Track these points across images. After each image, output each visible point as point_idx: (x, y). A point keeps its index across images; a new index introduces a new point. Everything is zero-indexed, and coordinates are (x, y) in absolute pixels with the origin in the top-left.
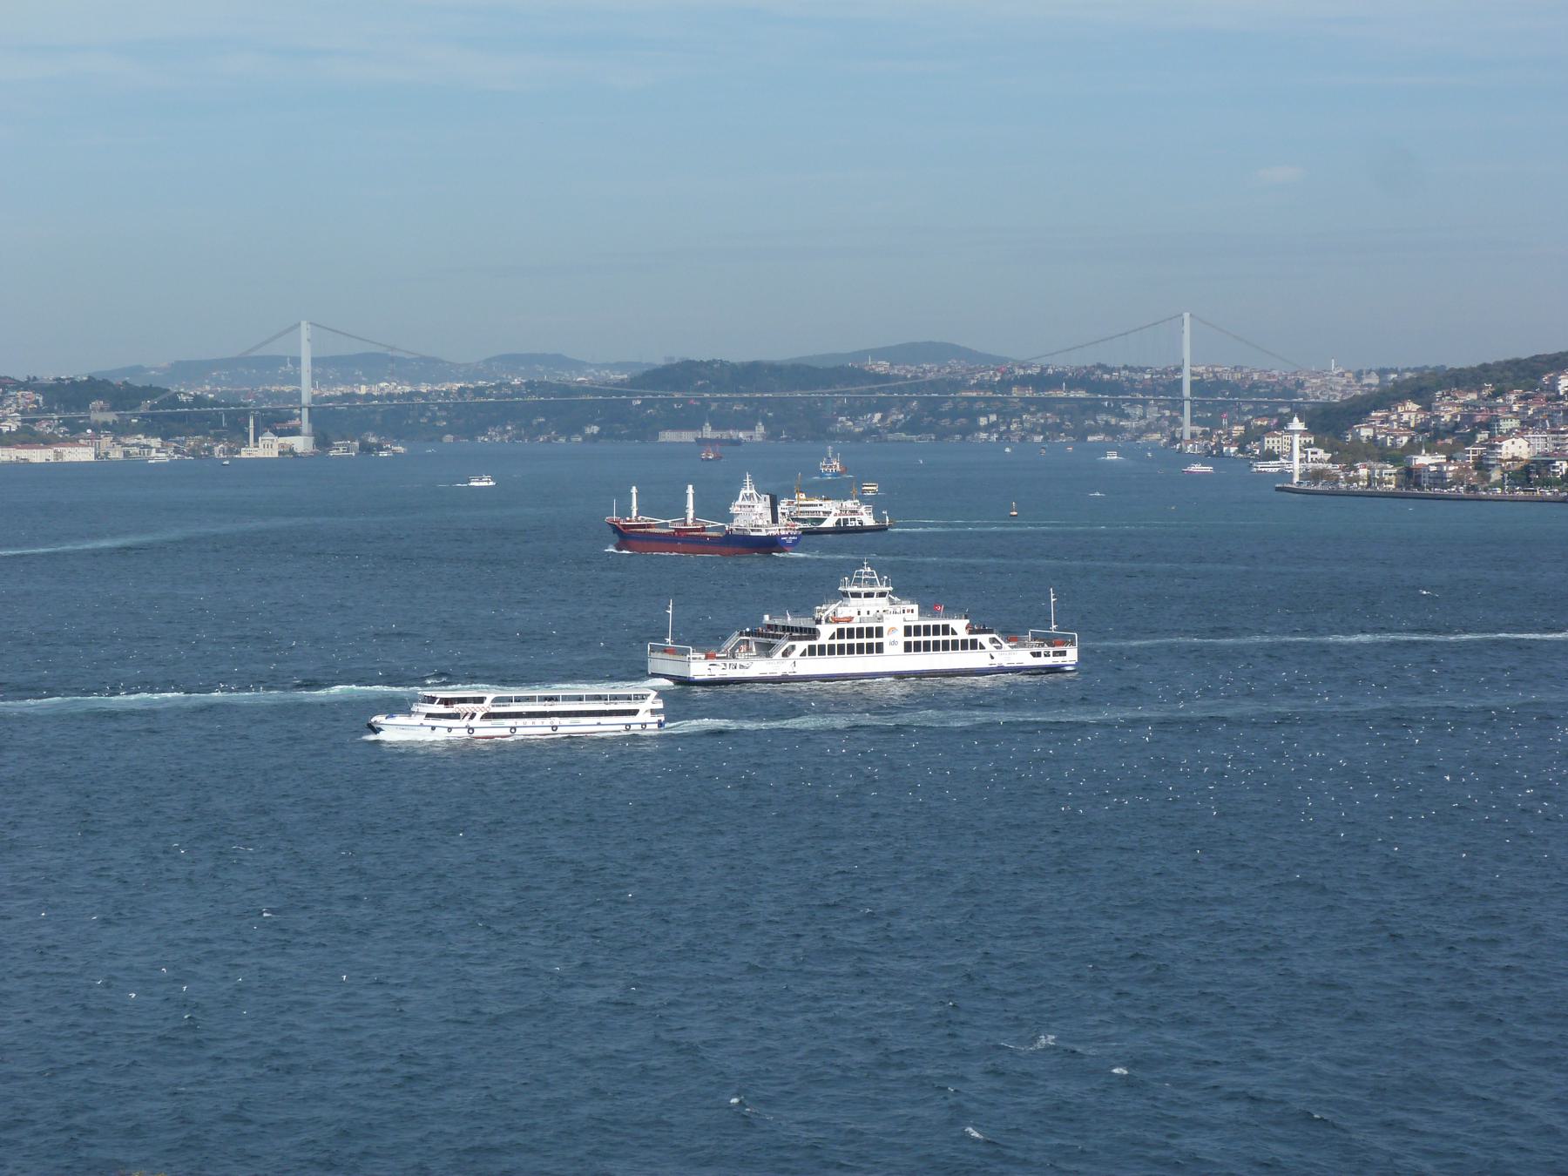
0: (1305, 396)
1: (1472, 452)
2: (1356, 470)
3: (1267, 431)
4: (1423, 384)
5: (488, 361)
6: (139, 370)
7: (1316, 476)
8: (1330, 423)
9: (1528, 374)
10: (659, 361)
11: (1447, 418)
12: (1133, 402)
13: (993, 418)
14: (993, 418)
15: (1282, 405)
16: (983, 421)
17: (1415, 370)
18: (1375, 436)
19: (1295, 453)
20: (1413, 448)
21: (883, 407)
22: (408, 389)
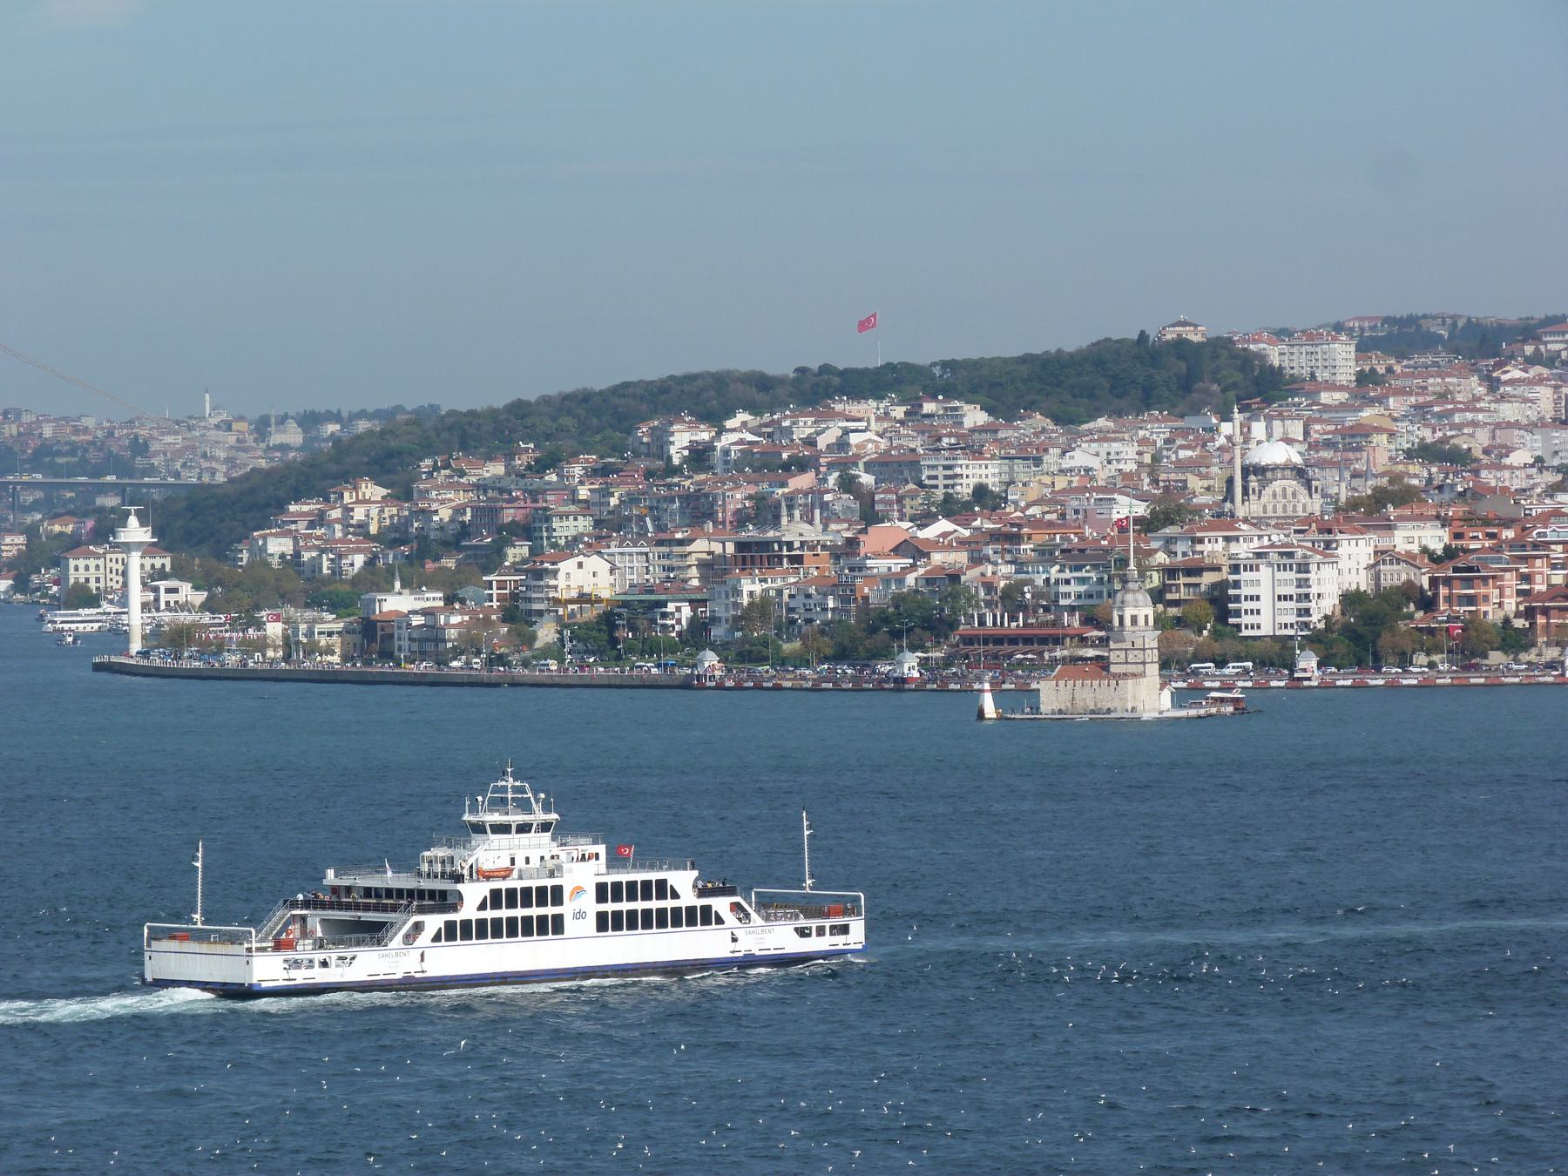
0: (151, 471)
1: (497, 586)
2: (260, 625)
3: (74, 544)
4: (394, 444)
7: (177, 638)
8: (202, 528)
9: (606, 422)
11: (445, 514)
15: (105, 489)
17: (377, 415)
18: (297, 554)
19: (134, 589)
20: (376, 578)
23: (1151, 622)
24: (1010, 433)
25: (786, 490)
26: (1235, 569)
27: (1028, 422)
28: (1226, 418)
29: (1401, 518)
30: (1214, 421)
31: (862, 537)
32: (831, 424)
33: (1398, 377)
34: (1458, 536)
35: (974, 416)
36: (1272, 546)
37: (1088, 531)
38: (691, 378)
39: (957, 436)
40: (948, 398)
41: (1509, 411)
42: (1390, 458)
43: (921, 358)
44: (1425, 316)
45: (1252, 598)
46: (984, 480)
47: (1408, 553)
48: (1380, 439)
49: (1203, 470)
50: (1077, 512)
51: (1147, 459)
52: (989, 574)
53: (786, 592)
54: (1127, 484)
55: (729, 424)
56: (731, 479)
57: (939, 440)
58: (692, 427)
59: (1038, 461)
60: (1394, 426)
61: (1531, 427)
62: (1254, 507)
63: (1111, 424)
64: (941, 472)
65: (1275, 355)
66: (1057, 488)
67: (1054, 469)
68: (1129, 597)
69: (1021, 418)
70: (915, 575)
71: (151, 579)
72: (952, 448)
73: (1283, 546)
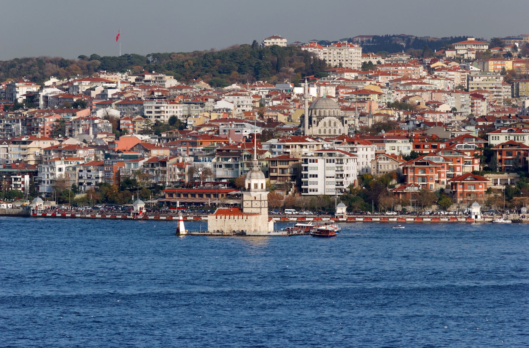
23: (264, 187)
24: (188, 90)
25: (75, 117)
26: (306, 161)
27: (198, 85)
28: (297, 85)
29: (387, 137)
30: (291, 86)
31: (116, 142)
32: (98, 84)
33: (382, 66)
34: (417, 147)
35: (170, 82)
36: (324, 150)
37: (231, 141)
38: (26, 60)
39: (162, 91)
40: (158, 72)
41: (439, 84)
42: (379, 107)
43: (143, 53)
44: (394, 36)
45: (313, 176)
46: (175, 114)
47: (393, 155)
48: (374, 97)
49: (286, 111)
50: (225, 131)
51: (257, 105)
52: (181, 161)
53: (78, 169)
54: (247, 118)
55: (47, 83)
56: (48, 111)
57: (153, 93)
58: (28, 84)
59: (202, 105)
60: (381, 91)
61: (450, 93)
62: (315, 130)
63: (239, 87)
64: (154, 110)
65: (321, 53)
66: (212, 119)
67: (211, 109)
68: (254, 174)
69: (194, 83)
70: (143, 161)
72: (159, 97)
73: (329, 150)
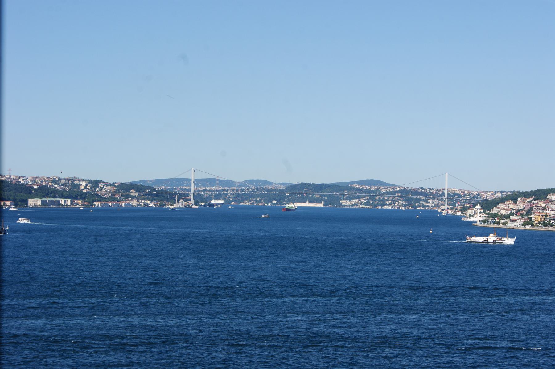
3: (469, 208)
5: (245, 181)
6: (145, 181)
7: (484, 222)
10: (295, 183)
12: (430, 198)
13: (390, 202)
14: (390, 202)
16: (387, 203)
21: (359, 198)
22: (221, 189)
71: (481, 213)
